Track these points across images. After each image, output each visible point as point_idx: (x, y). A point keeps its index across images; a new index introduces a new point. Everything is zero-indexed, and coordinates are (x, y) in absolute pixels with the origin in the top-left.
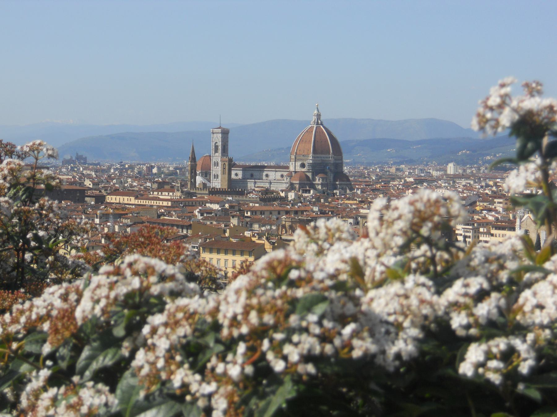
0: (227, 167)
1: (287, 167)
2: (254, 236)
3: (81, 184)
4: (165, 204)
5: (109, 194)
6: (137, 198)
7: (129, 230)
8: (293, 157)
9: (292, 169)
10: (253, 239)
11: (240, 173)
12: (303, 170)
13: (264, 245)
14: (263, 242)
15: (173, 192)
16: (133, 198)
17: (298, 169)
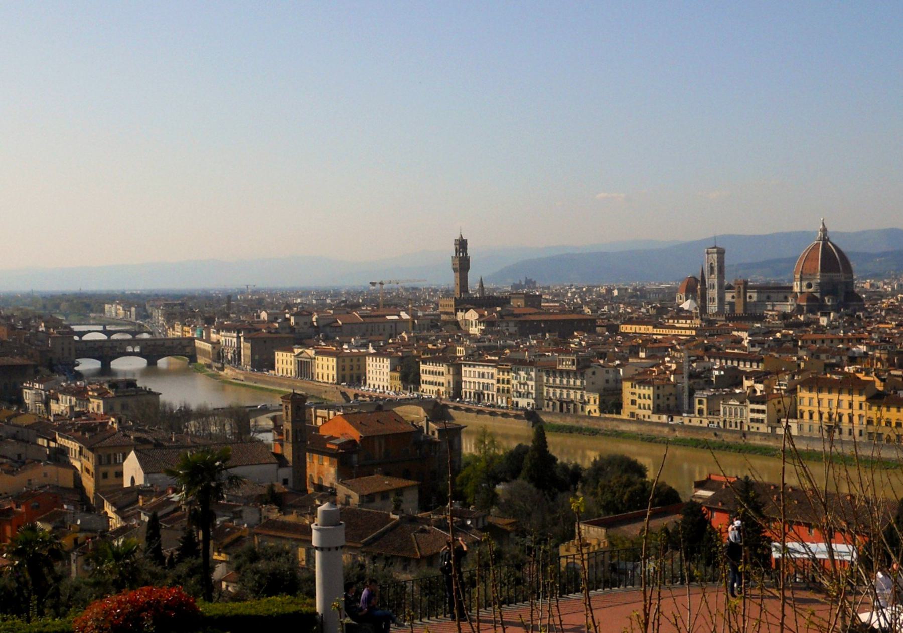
0: (742, 291)
1: (791, 288)
2: (857, 371)
3: (582, 312)
4: (688, 332)
5: (623, 323)
6: (655, 327)
7: (694, 365)
8: (798, 276)
9: (796, 289)
10: (859, 375)
11: (755, 296)
12: (810, 290)
13: (874, 382)
14: (871, 379)
15: (691, 318)
16: (650, 327)
17: (805, 289)
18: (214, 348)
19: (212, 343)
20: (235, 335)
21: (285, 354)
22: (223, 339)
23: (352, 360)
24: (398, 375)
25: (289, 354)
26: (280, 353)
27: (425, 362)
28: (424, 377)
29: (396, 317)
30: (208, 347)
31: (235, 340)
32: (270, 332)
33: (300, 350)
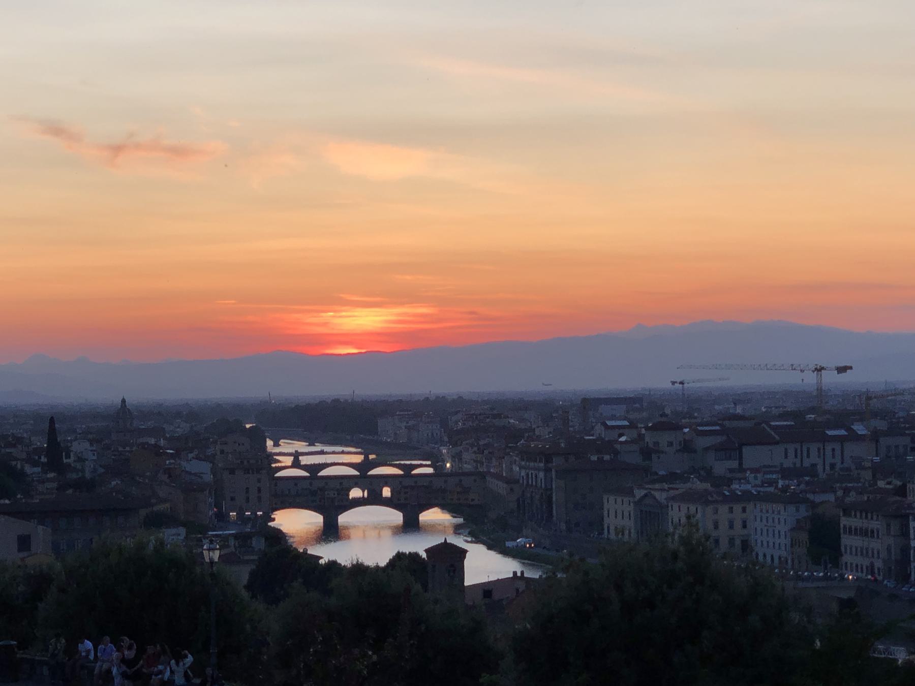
18: (512, 489)
19: (508, 481)
20: (542, 465)
21: (619, 500)
22: (523, 473)
23: (731, 510)
24: (804, 537)
25: (626, 499)
26: (612, 498)
27: (847, 512)
28: (847, 541)
29: (843, 432)
30: (500, 488)
31: (541, 475)
32: (600, 460)
33: (643, 492)
